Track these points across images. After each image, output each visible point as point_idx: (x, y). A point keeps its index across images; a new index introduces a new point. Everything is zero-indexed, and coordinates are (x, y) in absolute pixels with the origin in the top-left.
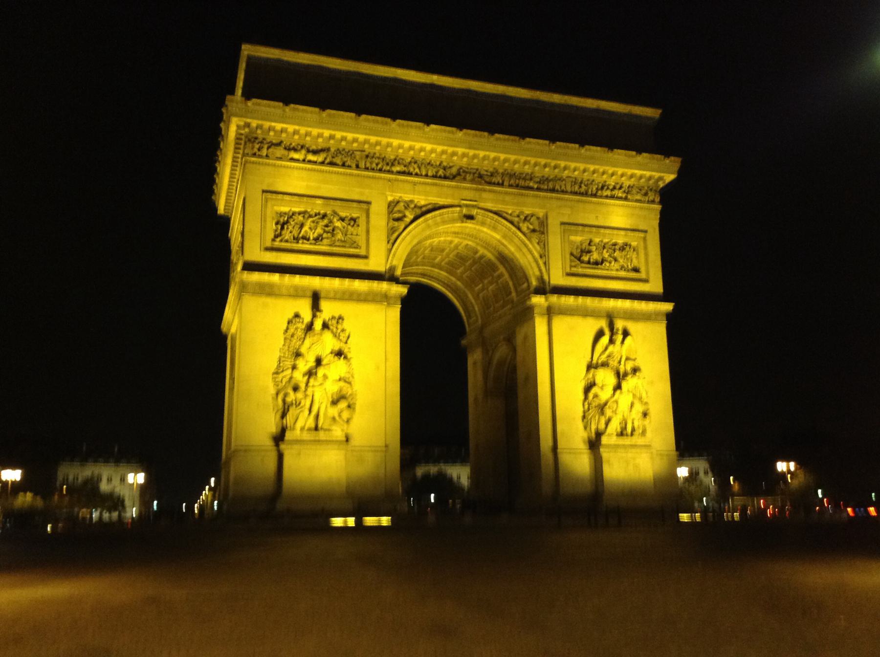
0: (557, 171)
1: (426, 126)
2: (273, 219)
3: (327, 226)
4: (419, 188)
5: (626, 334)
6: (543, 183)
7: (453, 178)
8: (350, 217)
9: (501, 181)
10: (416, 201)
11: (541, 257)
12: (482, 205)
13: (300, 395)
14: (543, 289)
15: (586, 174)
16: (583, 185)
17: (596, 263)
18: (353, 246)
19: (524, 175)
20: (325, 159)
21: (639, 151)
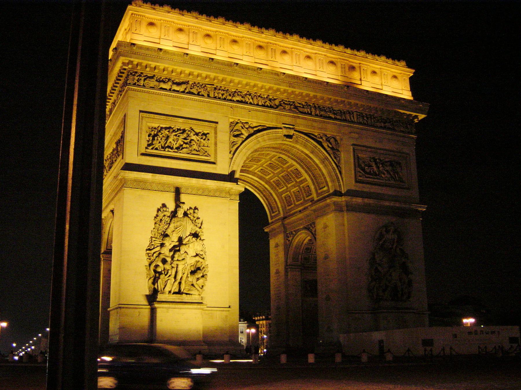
2: (147, 132)
3: (185, 139)
7: (276, 107)
8: (202, 133)
9: (310, 112)
10: (250, 123)
12: (297, 128)
13: (167, 267)
18: (204, 155)
20: (185, 89)
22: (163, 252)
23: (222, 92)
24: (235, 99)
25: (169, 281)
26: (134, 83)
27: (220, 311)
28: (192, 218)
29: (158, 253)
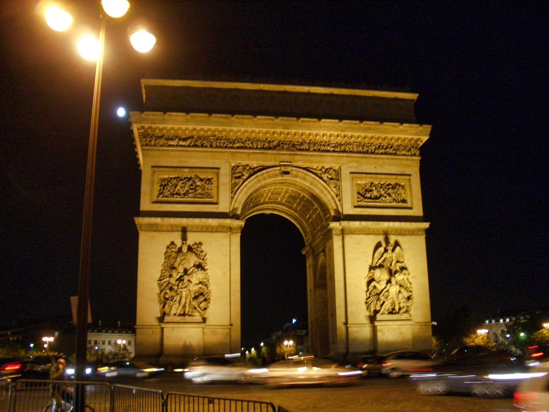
0: (346, 138)
1: (253, 118)
2: (158, 183)
3: (191, 185)
4: (251, 156)
5: (397, 244)
6: (337, 147)
7: (274, 148)
8: (207, 178)
9: (308, 148)
10: (250, 165)
11: (337, 196)
12: (294, 164)
14: (339, 217)
15: (366, 139)
16: (365, 147)
17: (376, 198)
19: (324, 143)
20: (191, 143)
21: (402, 122)
22: (171, 282)
23: (224, 141)
24: (236, 145)
25: (174, 305)
26: (147, 143)
27: (223, 328)
28: (196, 252)
29: (167, 283)
